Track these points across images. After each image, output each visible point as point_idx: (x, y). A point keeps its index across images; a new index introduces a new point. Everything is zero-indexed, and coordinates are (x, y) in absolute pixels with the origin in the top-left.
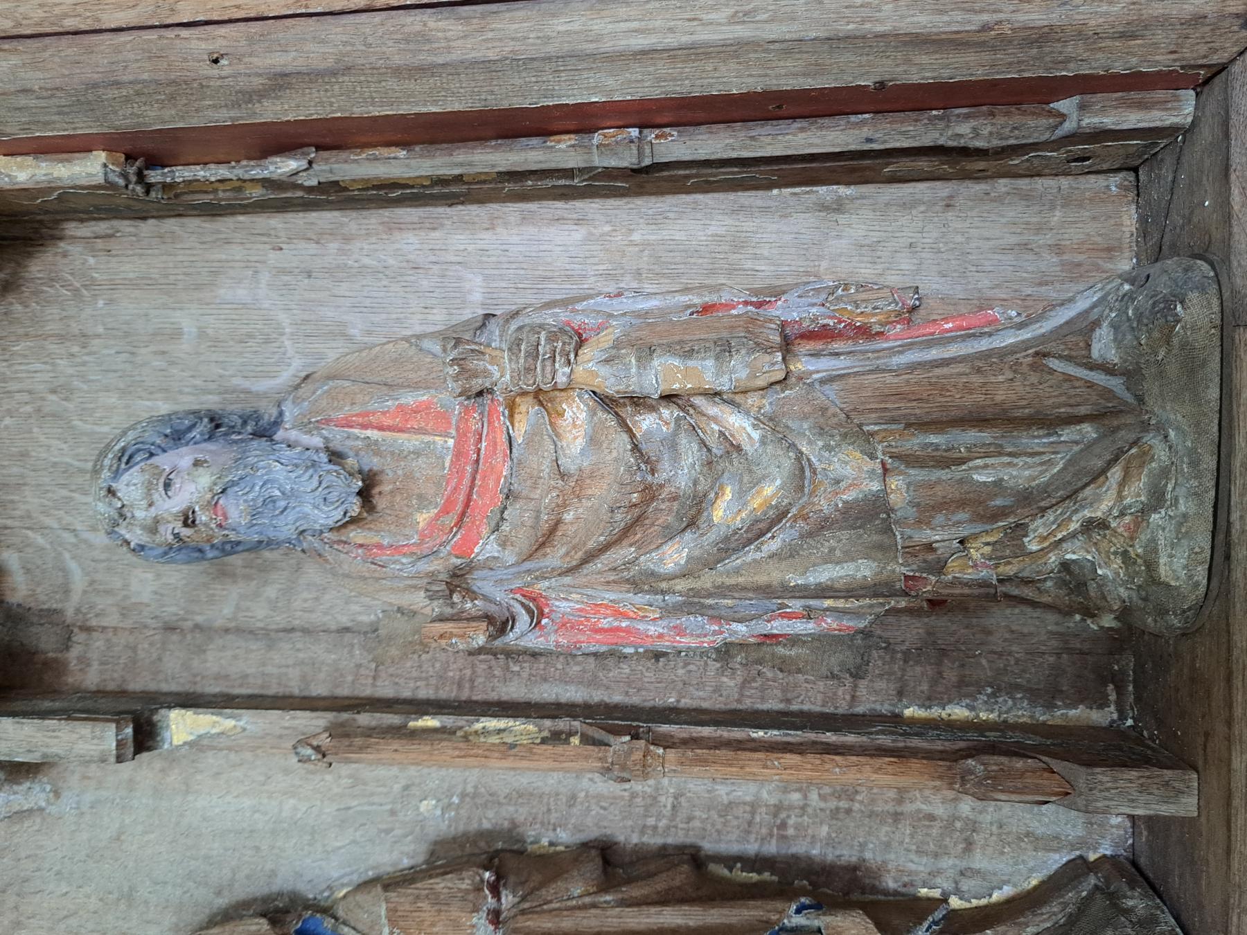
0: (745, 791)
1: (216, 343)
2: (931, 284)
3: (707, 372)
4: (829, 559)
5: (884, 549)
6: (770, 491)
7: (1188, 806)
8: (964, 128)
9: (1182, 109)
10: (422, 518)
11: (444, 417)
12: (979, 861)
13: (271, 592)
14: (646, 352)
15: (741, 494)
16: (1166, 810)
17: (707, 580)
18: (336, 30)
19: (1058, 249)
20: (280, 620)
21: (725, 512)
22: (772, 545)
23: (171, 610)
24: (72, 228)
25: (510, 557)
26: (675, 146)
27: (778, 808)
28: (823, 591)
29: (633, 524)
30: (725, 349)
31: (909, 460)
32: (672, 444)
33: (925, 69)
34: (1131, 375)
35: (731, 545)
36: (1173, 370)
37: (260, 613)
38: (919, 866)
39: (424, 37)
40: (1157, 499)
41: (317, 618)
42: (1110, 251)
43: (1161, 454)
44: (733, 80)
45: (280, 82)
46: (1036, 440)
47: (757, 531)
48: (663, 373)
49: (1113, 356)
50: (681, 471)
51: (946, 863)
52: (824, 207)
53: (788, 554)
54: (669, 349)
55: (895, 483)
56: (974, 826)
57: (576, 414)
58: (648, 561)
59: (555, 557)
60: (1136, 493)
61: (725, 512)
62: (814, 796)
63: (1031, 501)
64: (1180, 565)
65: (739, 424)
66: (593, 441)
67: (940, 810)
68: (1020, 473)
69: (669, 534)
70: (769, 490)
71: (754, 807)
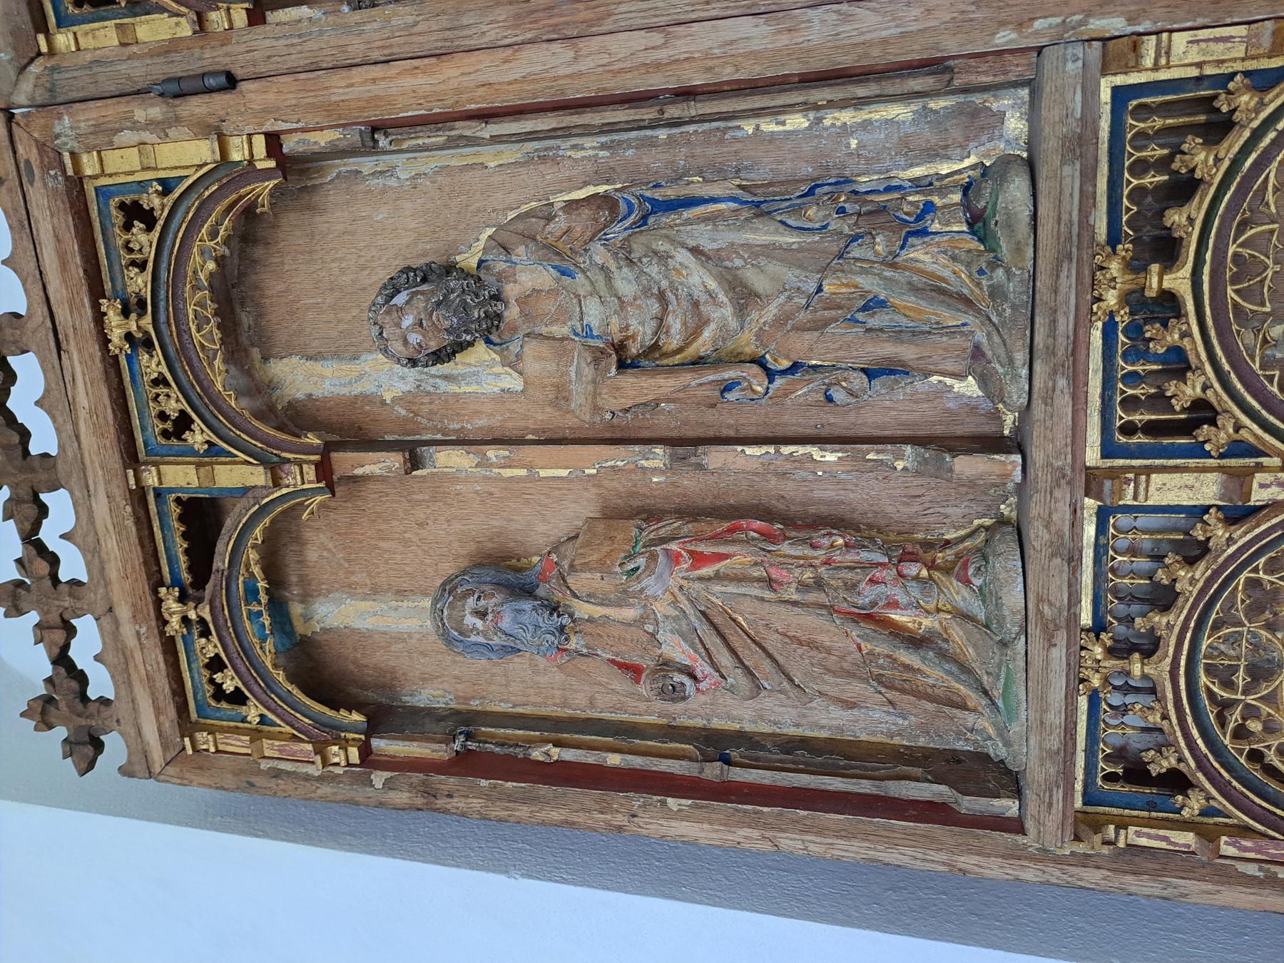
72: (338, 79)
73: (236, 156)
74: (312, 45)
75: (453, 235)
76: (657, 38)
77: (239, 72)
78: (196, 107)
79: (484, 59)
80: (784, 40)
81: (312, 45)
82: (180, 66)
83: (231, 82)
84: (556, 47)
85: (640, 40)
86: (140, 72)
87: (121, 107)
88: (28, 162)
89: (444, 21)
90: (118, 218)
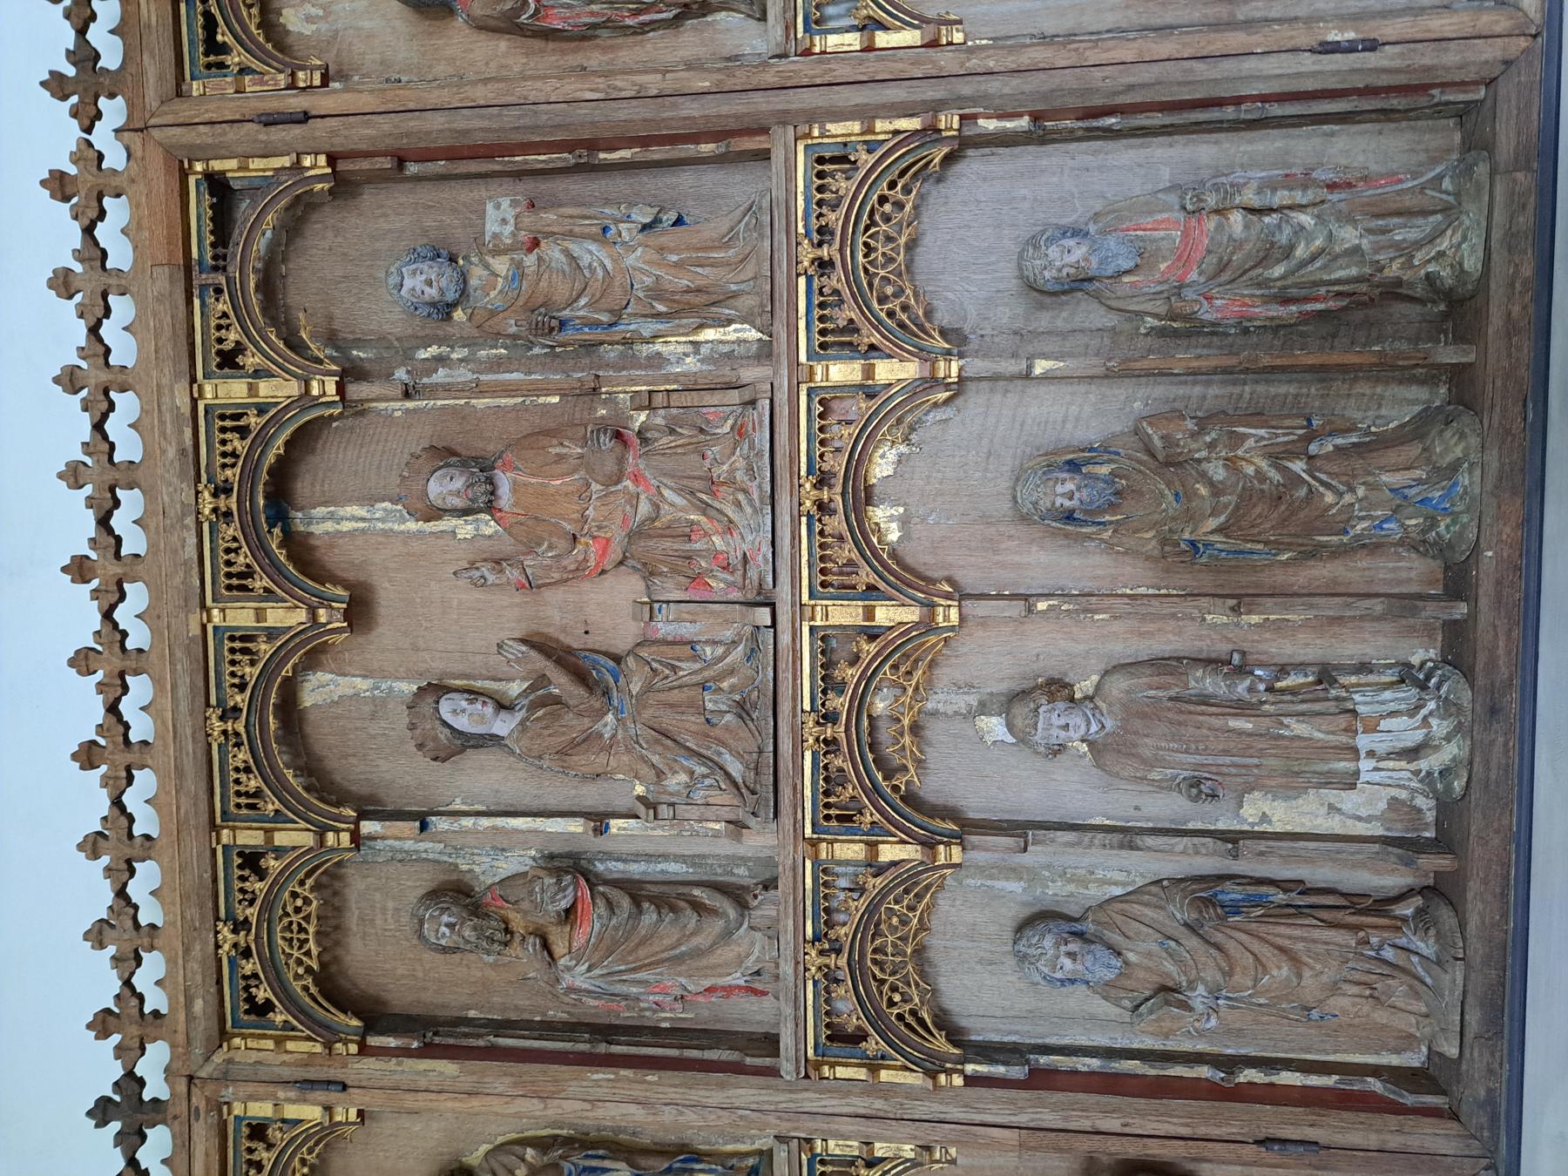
0: (1283, 389)
1: (1042, 202)
2: (1374, 167)
3: (1299, 197)
4: (1341, 268)
5: (1362, 263)
6: (1318, 243)
7: (1471, 358)
8: (1395, 102)
9: (1482, 93)
10: (1163, 266)
11: (1178, 222)
12: (1384, 412)
13: (1064, 314)
14: (1274, 190)
15: (1307, 244)
16: (1463, 360)
17: (1289, 282)
18: (1156, 68)
19: (1427, 151)
20: (1069, 327)
21: (1300, 252)
22: (1318, 264)
23: (1018, 325)
24: (970, 152)
25: (1202, 280)
26: (1276, 110)
27: (1296, 396)
28: (1338, 282)
29: (1265, 259)
30: (1305, 188)
31: (1370, 231)
32: (1279, 226)
33: (1384, 80)
34: (1457, 195)
35: (1304, 264)
36: (1472, 191)
37: (1059, 323)
38: (1358, 415)
39: (1191, 70)
40: (1464, 238)
41: (1087, 325)
42: (1449, 151)
43: (1467, 222)
44: (1310, 85)
45: (1131, 88)
46: (1420, 221)
47: (1314, 258)
48: (1281, 197)
49: (1450, 188)
50: (1283, 238)
51: (1370, 413)
52: (1325, 134)
53: (1324, 268)
54: (1283, 187)
55: (1365, 241)
56: (1382, 397)
57: (1237, 218)
58: (1267, 274)
59: (1225, 277)
60: (1457, 238)
61: (1300, 252)
62: (1313, 390)
63: (1418, 245)
64: (1472, 264)
65: (1306, 219)
66: (1246, 227)
67: (1368, 392)
68: (1413, 235)
69: (1278, 261)
70: (1318, 243)
71: (1286, 396)
72: (408, 1096)
73: (338, 1118)
74: (396, 1077)
75: (461, 1145)
76: (588, 1106)
77: (349, 1083)
78: (320, 1095)
79: (495, 1101)
80: (651, 1118)
81: (396, 1077)
82: (312, 1074)
83: (345, 1087)
84: (535, 1101)
85: (578, 1105)
86: (286, 1073)
87: (271, 1088)
88: (197, 1108)
89: (475, 1078)
90: (245, 1131)
